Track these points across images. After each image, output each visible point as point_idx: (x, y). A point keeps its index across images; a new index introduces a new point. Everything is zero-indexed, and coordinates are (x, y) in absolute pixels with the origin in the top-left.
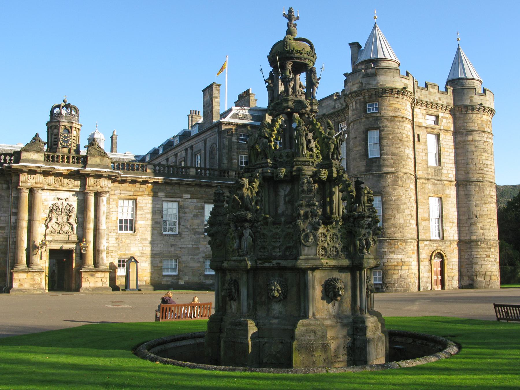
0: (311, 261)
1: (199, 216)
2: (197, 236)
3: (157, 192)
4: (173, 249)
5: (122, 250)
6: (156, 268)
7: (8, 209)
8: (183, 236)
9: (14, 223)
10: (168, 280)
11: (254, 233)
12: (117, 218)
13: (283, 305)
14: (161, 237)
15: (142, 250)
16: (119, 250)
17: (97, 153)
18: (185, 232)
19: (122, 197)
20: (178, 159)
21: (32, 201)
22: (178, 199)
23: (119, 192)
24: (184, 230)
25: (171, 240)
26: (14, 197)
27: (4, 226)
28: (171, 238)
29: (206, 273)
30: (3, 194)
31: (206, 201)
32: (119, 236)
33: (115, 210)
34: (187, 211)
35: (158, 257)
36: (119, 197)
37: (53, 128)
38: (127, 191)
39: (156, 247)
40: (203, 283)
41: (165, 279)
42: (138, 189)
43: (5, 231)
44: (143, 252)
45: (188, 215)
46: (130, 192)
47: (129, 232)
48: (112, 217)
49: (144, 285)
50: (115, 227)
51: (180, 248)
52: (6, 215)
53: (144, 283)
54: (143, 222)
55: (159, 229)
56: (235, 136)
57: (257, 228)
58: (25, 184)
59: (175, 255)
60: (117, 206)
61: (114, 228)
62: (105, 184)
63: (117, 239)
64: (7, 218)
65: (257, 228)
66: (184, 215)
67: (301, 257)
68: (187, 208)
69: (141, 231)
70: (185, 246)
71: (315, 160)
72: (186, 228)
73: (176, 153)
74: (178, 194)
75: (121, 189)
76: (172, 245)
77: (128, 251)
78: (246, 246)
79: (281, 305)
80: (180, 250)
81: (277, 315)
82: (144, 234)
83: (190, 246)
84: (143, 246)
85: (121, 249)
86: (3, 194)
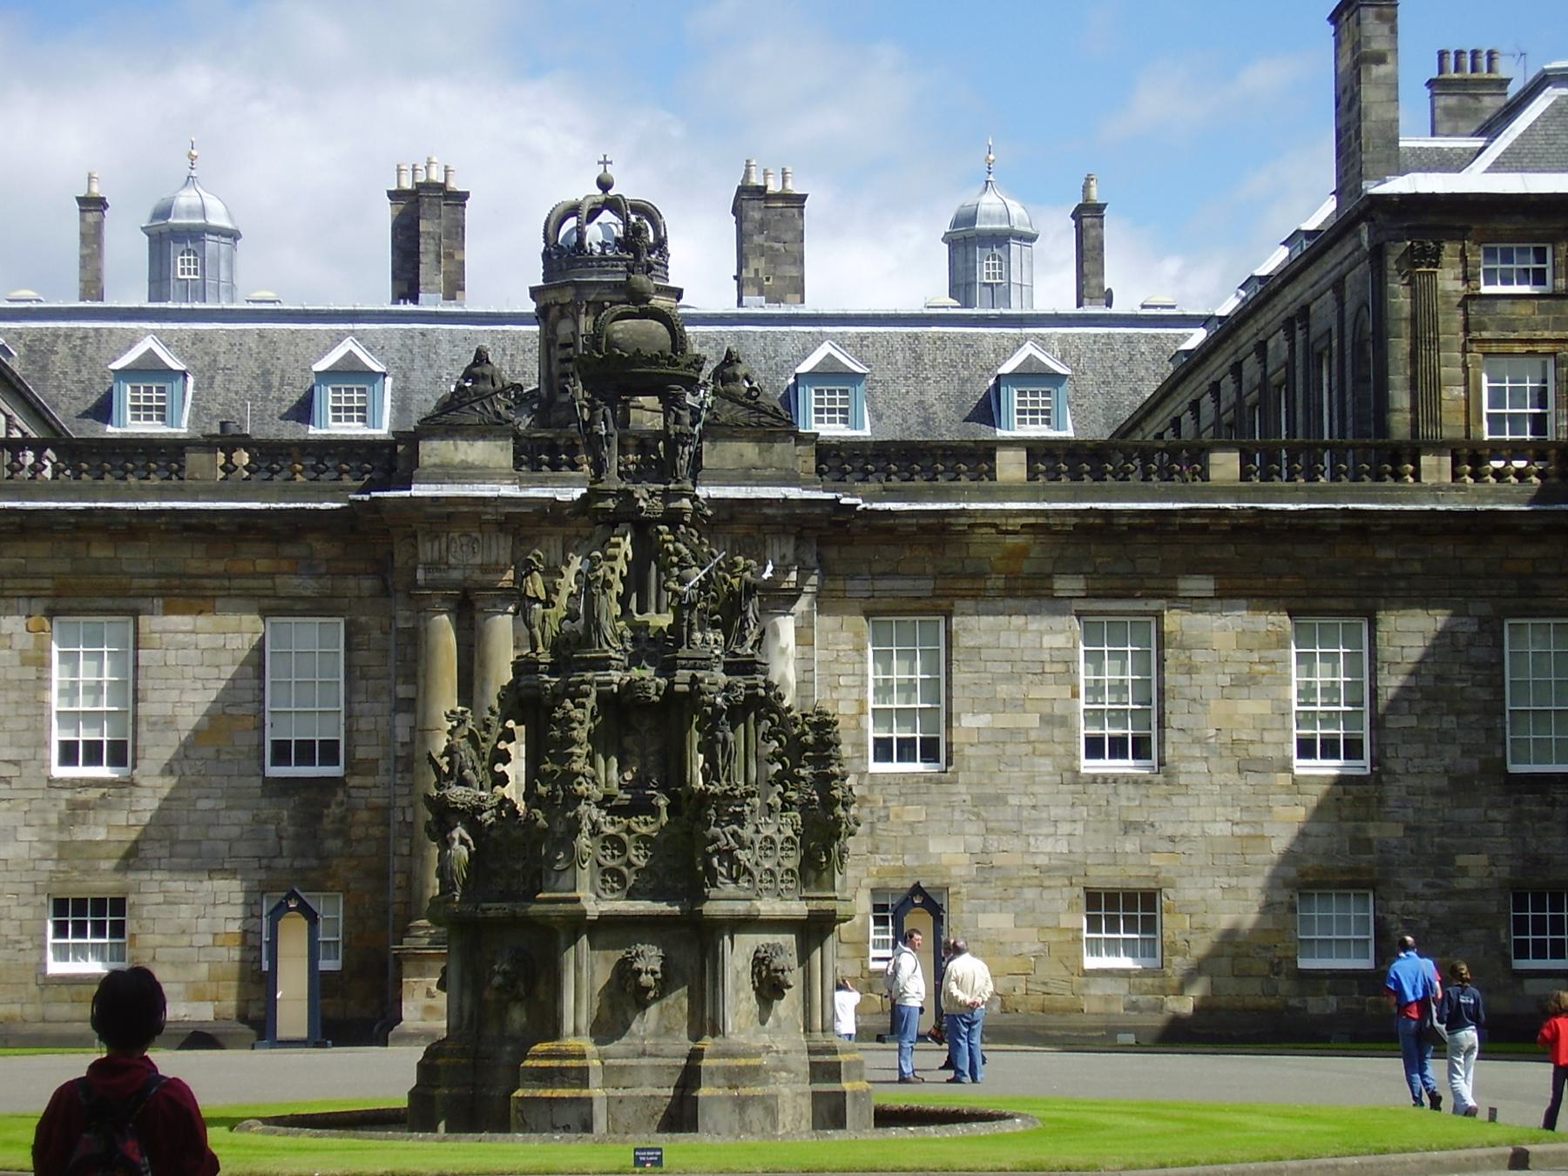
1: (1265, 680)
2: (1253, 778)
3: (1050, 576)
4: (1130, 845)
6: (1053, 937)
8: (1183, 780)
9: (403, 744)
10: (1109, 992)
12: (862, 703)
14: (1072, 787)
16: (874, 850)
18: (1194, 758)
20: (1270, 370)
21: (472, 646)
22: (1154, 605)
23: (867, 585)
24: (1186, 752)
25: (1124, 803)
27: (373, 756)
28: (1122, 789)
29: (1304, 964)
30: (363, 619)
31: (1299, 604)
33: (848, 668)
34: (1199, 657)
35: (1059, 882)
38: (904, 576)
39: (1048, 836)
40: (1289, 1009)
41: (1099, 988)
44: (985, 858)
45: (1202, 678)
46: (920, 583)
47: (918, 767)
50: (854, 745)
51: (1172, 839)
52: (377, 707)
54: (983, 720)
55: (1061, 750)
56: (1452, 266)
59: (1145, 872)
66: (1183, 680)
68: (1205, 645)
69: (973, 764)
70: (1196, 831)
72: (1197, 741)
73: (1261, 337)
74: (1151, 576)
75: (877, 568)
76: (1128, 827)
77: (918, 857)
80: (1170, 846)
82: (991, 776)
83: (1221, 829)
85: (883, 846)
86: (363, 619)
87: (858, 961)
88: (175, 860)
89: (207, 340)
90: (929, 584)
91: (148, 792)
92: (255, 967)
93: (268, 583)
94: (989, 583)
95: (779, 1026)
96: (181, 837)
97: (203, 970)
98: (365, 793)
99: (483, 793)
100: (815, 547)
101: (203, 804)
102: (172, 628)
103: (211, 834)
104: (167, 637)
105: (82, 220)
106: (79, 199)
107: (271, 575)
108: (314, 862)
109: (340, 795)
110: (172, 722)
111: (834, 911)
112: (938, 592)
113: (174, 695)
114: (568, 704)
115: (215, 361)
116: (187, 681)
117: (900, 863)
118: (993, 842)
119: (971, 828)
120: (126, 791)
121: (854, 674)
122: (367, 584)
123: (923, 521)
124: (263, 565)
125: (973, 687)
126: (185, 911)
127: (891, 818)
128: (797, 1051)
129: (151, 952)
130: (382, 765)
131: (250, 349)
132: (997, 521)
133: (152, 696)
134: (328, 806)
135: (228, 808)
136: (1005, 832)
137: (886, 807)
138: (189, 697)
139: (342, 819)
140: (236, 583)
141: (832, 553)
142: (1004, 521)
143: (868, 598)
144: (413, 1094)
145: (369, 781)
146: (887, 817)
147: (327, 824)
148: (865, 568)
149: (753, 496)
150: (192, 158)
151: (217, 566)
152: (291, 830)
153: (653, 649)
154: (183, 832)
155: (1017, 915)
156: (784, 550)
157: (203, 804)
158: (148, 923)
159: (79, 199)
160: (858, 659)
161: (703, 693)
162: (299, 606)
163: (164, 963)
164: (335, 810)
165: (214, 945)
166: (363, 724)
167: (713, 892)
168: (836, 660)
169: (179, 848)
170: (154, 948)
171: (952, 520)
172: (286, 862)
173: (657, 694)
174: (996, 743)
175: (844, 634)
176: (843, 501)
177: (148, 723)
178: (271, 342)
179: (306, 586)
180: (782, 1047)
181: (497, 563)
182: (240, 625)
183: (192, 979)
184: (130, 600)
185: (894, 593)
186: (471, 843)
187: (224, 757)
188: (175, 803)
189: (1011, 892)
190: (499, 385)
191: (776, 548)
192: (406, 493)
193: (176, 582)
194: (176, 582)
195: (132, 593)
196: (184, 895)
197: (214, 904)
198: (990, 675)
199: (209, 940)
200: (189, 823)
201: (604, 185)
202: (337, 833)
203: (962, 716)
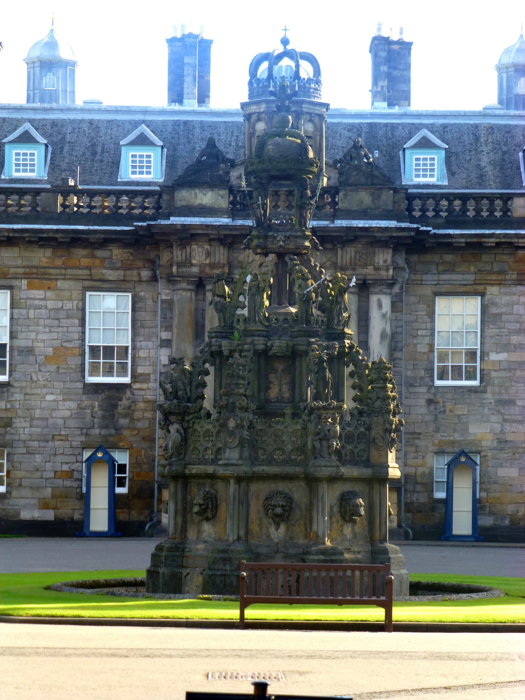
0: (231, 468)
5: (444, 432)
7: (154, 330)
9: (164, 366)
11: (185, 430)
13: (212, 525)
15: (502, 432)
16: (437, 430)
17: (363, 180)
19: (444, 289)
23: (436, 277)
26: (163, 301)
27: (147, 372)
32: (435, 395)
33: (424, 326)
36: (437, 289)
37: (254, 118)
42: (488, 268)
43: (151, 385)
44: (503, 437)
48: (415, 345)
49: (507, 527)
50: (425, 370)
52: (150, 344)
53: (507, 522)
54: (503, 356)
57: (188, 422)
58: (185, 269)
60: (431, 314)
61: (422, 373)
62: (385, 261)
63: (430, 402)
64: (153, 352)
65: (188, 422)
67: (220, 462)
69: (496, 382)
71: (280, 326)
78: (170, 446)
79: (210, 525)
81: (206, 539)
82: (507, 389)
84: (505, 420)
85: (442, 428)
86: (142, 294)
87: (426, 494)
88: (33, 429)
89: (59, 125)
90: (472, 277)
91: (18, 390)
92: (78, 490)
93: (86, 272)
94: (508, 277)
95: (355, 537)
96: (36, 416)
97: (48, 492)
98: (143, 393)
99: (189, 404)
100: (404, 255)
101: (49, 398)
102: (33, 296)
103: (54, 415)
104: (29, 302)
107: (89, 268)
108: (113, 431)
109: (128, 394)
110: (32, 351)
112: (477, 282)
113: (33, 335)
114: (236, 355)
115: (64, 138)
116: (41, 328)
117: (452, 438)
118: (508, 427)
119: (494, 418)
120: (5, 389)
121: (426, 329)
122: (146, 274)
123: (469, 240)
124: (85, 262)
125: (497, 337)
126: (38, 458)
127: (447, 412)
129: (18, 481)
130: (152, 377)
131: (84, 131)
132: (513, 240)
133: (21, 336)
134: (121, 400)
135: (64, 400)
136: (515, 421)
137: (444, 406)
138: (40, 337)
139: (129, 407)
140: (69, 272)
141: (414, 258)
142: (516, 240)
143: (436, 285)
144: (149, 572)
145: (145, 386)
146: (445, 412)
147: (120, 409)
148: (434, 267)
149: (367, 226)
151: (59, 262)
152: (100, 413)
153: (286, 325)
154: (38, 413)
155: (520, 469)
156: (385, 258)
157: (49, 398)
158: (17, 465)
160: (429, 320)
161: (313, 351)
162: (106, 285)
163: (26, 487)
164: (124, 402)
165: (55, 478)
166: (142, 354)
168: (416, 321)
169: (35, 422)
170: (21, 479)
171: (486, 240)
172: (97, 431)
174: (509, 370)
175: (420, 306)
176: (422, 228)
177: (18, 351)
178: (97, 127)
179: (111, 275)
181: (219, 263)
182: (71, 295)
183: (42, 497)
184: (8, 280)
185: (451, 282)
186: (182, 431)
187: (61, 371)
188: (33, 396)
189: (517, 456)
190: (221, 159)
191: (381, 256)
193: (35, 271)
194: (35, 271)
195: (9, 276)
196: (39, 449)
197: (55, 455)
198: (506, 330)
199: (52, 475)
200: (41, 408)
201: (285, 42)
202: (125, 416)
203: (490, 354)
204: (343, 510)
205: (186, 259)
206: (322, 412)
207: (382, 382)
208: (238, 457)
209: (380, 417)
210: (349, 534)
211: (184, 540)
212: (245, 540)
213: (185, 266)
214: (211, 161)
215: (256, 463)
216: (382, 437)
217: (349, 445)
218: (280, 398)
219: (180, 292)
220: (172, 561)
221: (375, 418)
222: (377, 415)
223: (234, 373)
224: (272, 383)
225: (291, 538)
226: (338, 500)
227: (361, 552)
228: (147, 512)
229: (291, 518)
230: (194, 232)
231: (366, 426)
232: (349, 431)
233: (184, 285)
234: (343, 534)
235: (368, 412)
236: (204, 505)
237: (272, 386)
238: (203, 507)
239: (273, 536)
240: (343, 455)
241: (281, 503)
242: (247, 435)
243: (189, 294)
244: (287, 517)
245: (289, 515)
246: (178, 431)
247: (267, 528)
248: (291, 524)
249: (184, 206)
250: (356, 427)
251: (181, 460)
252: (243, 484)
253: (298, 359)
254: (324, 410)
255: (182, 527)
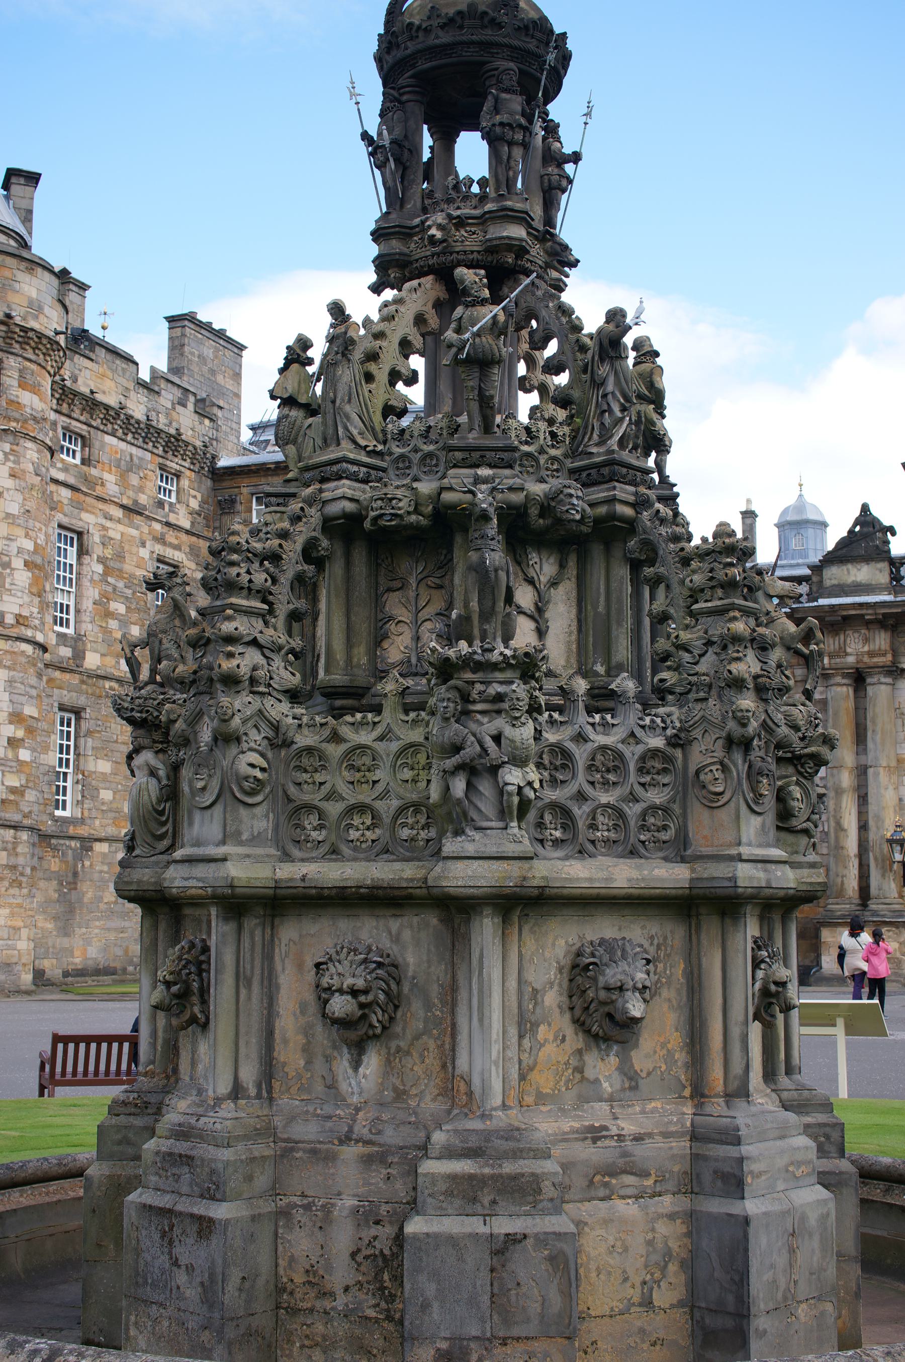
0: (200, 871)
58: (838, 660)
95: (634, 1088)
105: (743, 523)
106: (742, 513)
111: (734, 879)
128: (666, 1135)
150: (801, 485)
159: (742, 513)
167: (450, 846)
173: (416, 511)
180: (629, 1128)
181: (880, 649)
190: (877, 527)
192: (815, 604)
204: (578, 1003)
205: (840, 648)
206: (469, 676)
207: (720, 592)
208: (220, 836)
209: (711, 702)
210: (608, 1078)
211: (172, 1080)
212: (259, 1096)
213: (839, 656)
214: (865, 530)
215: (296, 853)
216: (721, 763)
217: (607, 791)
218: (414, 660)
219: (834, 688)
220: (120, 1143)
221: (699, 706)
222: (702, 695)
223: (219, 577)
224: (391, 618)
225: (400, 1095)
226: (560, 970)
227: (650, 1135)
228: (813, 955)
229: (398, 1029)
230: (845, 613)
231: (669, 732)
232: (603, 748)
233: (839, 679)
234: (583, 1078)
235: (678, 690)
236: (175, 984)
237: (392, 626)
238: (175, 989)
239: (344, 1087)
240: (581, 824)
241: (349, 981)
242: (252, 766)
243: (844, 689)
244: (384, 1028)
245: (391, 1019)
246: (153, 773)
247: (328, 1059)
248: (398, 1046)
249: (834, 585)
250: (633, 734)
251: (161, 853)
252: (250, 923)
253: (458, 539)
254: (474, 673)
255: (166, 1042)
